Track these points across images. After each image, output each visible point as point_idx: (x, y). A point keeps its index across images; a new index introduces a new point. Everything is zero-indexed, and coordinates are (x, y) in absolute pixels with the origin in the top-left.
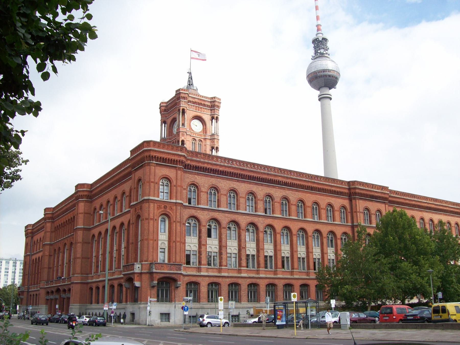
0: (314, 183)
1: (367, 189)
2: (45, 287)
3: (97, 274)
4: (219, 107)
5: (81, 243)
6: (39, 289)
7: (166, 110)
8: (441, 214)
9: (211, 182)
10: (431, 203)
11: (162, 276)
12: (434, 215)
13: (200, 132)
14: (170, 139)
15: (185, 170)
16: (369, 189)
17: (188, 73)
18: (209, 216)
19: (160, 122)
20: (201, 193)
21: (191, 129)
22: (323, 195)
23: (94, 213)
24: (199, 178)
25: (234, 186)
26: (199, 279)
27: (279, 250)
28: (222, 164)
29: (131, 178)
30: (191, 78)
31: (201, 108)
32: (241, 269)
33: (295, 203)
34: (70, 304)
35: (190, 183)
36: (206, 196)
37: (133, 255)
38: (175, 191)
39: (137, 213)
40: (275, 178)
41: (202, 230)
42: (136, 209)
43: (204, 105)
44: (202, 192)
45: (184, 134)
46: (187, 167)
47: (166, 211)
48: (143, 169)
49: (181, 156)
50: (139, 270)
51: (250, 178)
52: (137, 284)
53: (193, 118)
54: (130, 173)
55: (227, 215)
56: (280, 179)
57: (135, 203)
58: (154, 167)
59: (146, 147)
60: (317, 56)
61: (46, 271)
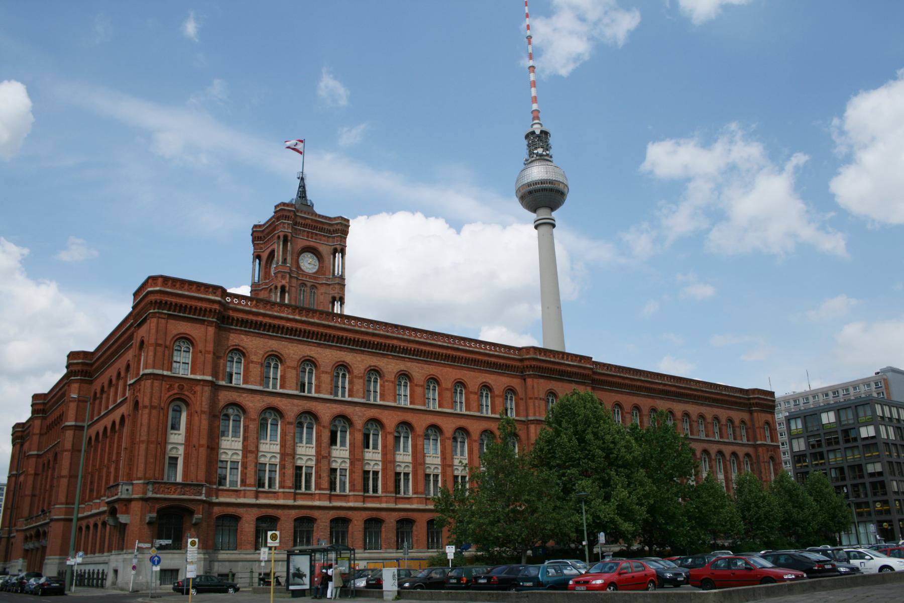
1: (552, 360)
2: (24, 528)
4: (345, 233)
7: (261, 237)
9: (270, 348)
10: (669, 383)
12: (674, 403)
13: (314, 273)
14: (266, 284)
15: (222, 325)
16: (557, 360)
17: (299, 178)
18: (264, 403)
20: (251, 365)
25: (312, 352)
27: (390, 462)
31: (316, 234)
33: (421, 383)
34: (46, 557)
36: (260, 370)
41: (251, 426)
43: (321, 230)
44: (252, 362)
45: (286, 276)
47: (181, 394)
49: (214, 302)
51: (340, 340)
55: (296, 401)
59: (151, 286)
60: (533, 159)
61: (27, 500)
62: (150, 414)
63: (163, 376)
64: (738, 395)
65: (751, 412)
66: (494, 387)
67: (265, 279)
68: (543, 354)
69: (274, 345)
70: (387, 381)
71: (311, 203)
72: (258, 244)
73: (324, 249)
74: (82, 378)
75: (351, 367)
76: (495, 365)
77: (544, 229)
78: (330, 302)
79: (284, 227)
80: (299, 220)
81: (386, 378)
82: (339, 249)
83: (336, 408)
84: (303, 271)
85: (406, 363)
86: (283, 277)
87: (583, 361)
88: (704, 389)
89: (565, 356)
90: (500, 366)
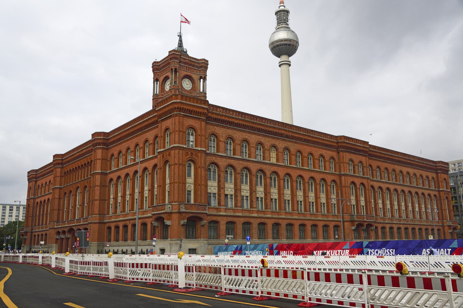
0: (310, 136)
1: (352, 143)
2: (55, 227)
3: (116, 214)
4: (206, 68)
5: (98, 186)
6: (48, 229)
7: (158, 69)
8: (409, 167)
11: (191, 215)
12: (403, 167)
13: (190, 90)
14: (162, 95)
17: (178, 36)
19: (153, 79)
20: (220, 142)
21: (182, 86)
23: (111, 159)
24: (218, 129)
26: (219, 218)
28: (237, 117)
29: (157, 127)
30: (181, 41)
31: (191, 68)
32: (253, 210)
33: (294, 153)
35: (211, 133)
37: (161, 197)
38: (199, 140)
39: (166, 158)
40: (279, 131)
41: (221, 175)
42: (163, 155)
43: (194, 66)
44: (221, 141)
46: (209, 118)
48: (171, 119)
49: (204, 108)
50: (170, 210)
51: (259, 130)
52: (168, 222)
53: (184, 77)
54: (156, 122)
55: (241, 162)
56: (283, 132)
57: (162, 150)
58: (181, 118)
62: (179, 168)
63: (183, 147)
64: (431, 164)
66: (325, 156)
67: (162, 92)
68: (348, 140)
70: (280, 152)
71: (186, 50)
72: (156, 73)
73: (195, 77)
74: (103, 147)
75: (264, 144)
77: (284, 67)
79: (175, 64)
80: (182, 60)
82: (203, 77)
84: (184, 89)
85: (288, 143)
87: (365, 144)
88: (416, 160)
89: (357, 141)
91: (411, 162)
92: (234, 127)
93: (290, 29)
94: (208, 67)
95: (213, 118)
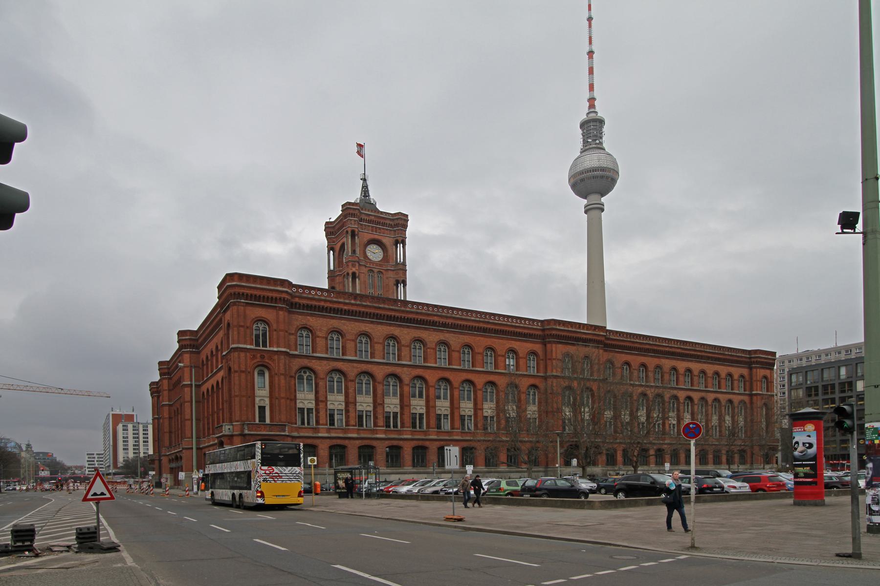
0: (488, 323)
1: (570, 329)
4: (405, 226)
8: (692, 361)
12: (679, 362)
14: (340, 271)
18: (330, 367)
21: (366, 257)
22: (502, 338)
25: (367, 328)
31: (380, 228)
33: (458, 349)
35: (300, 326)
40: (428, 318)
43: (383, 224)
44: (318, 337)
51: (389, 318)
55: (355, 365)
64: (740, 355)
65: (751, 369)
68: (561, 325)
69: (335, 323)
70: (429, 348)
71: (374, 201)
72: (331, 238)
73: (387, 241)
75: (399, 338)
76: (520, 335)
78: (394, 285)
79: (351, 223)
80: (363, 217)
81: (428, 346)
82: (400, 241)
83: (388, 369)
84: (370, 260)
86: (353, 266)
88: (708, 351)
89: (582, 326)
90: (525, 335)
91: (695, 353)
92: (342, 316)
93: (604, 150)
94: (407, 225)
95: (303, 304)
